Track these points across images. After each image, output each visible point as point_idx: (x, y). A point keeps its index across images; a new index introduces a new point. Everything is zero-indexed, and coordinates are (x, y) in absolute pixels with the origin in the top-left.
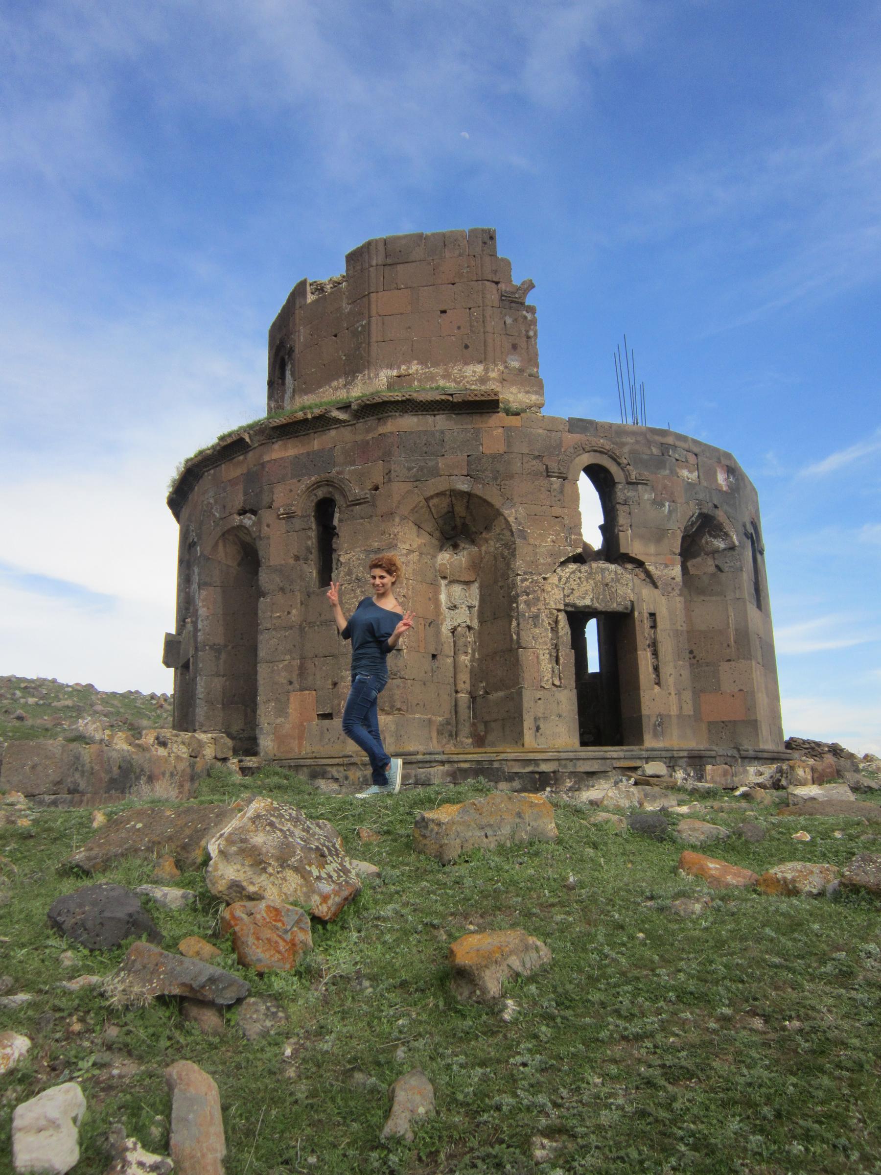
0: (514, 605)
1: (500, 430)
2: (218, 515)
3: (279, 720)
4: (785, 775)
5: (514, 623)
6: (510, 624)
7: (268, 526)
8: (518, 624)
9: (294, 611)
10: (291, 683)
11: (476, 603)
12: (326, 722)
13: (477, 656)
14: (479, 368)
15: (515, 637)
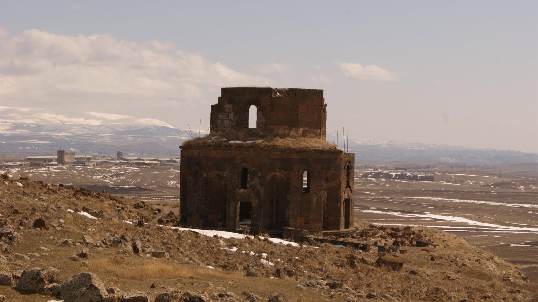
0: (339, 199)
1: (340, 159)
2: (269, 167)
3: (295, 224)
4: (364, 234)
5: (339, 204)
6: (338, 203)
7: (292, 176)
8: (340, 204)
9: (299, 198)
10: (298, 215)
11: (326, 196)
12: (307, 224)
13: (325, 208)
14: (320, 131)
15: (339, 207)
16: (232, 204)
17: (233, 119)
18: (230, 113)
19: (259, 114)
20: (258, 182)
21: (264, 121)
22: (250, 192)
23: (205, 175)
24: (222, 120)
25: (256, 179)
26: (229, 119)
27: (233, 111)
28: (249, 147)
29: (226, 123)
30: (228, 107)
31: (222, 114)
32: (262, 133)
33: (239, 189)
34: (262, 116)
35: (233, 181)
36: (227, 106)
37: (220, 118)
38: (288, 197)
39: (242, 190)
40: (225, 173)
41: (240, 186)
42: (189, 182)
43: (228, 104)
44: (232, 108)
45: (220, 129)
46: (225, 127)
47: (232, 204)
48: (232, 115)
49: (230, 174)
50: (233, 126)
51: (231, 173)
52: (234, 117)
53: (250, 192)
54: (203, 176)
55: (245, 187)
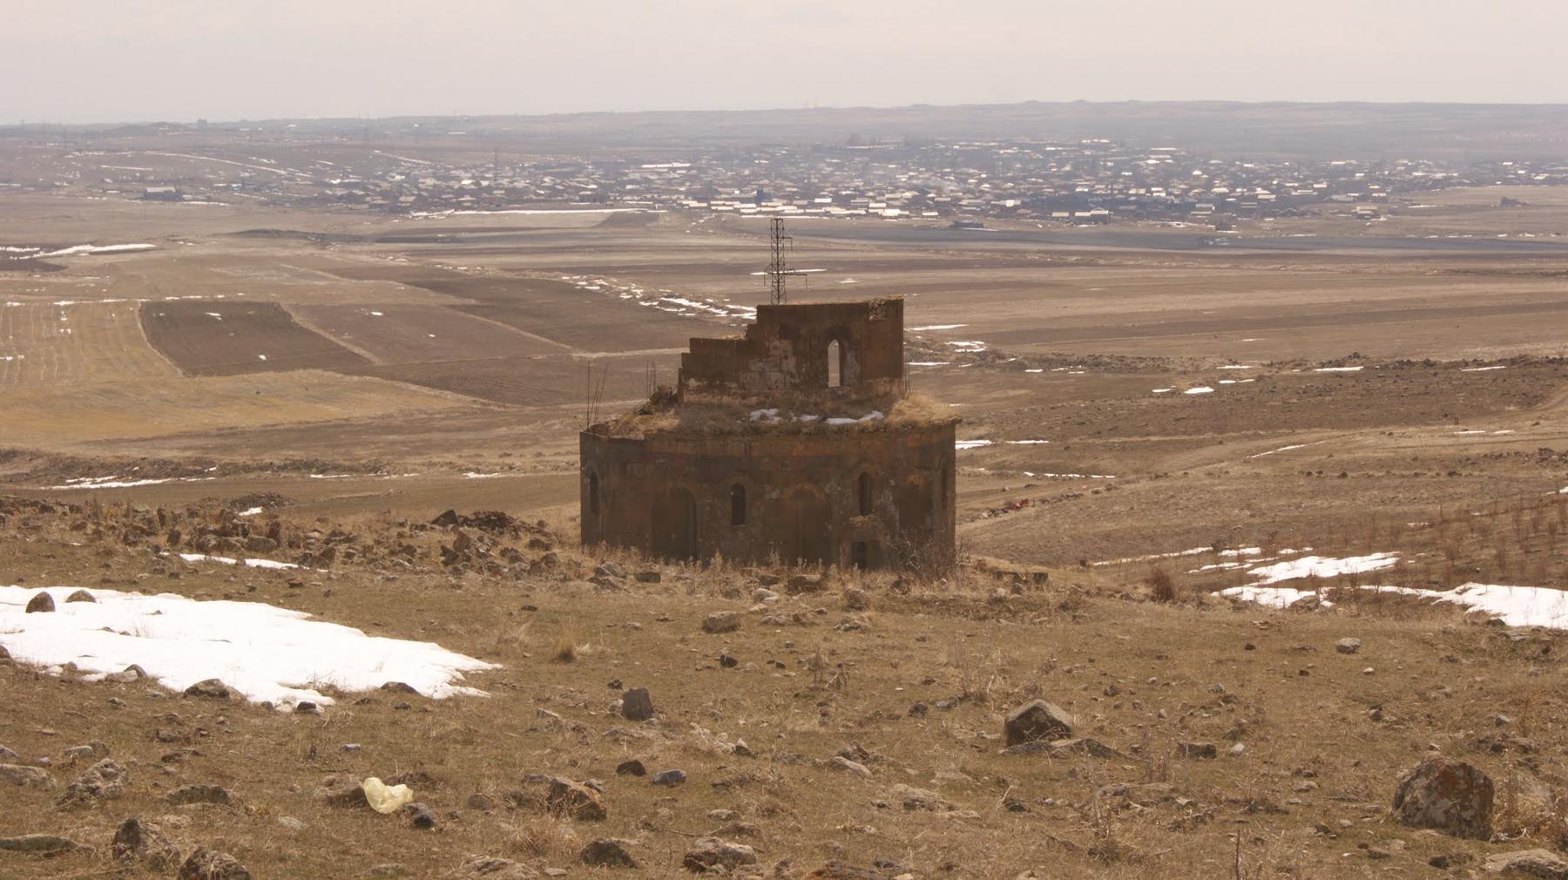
16: (844, 550)
17: (794, 371)
18: (786, 358)
19: (849, 356)
20: (891, 498)
21: (859, 370)
22: (875, 520)
23: (774, 495)
24: (761, 374)
25: (887, 492)
26: (781, 371)
27: (794, 354)
28: (877, 430)
29: (774, 379)
30: (779, 346)
31: (760, 361)
32: (854, 397)
33: (855, 516)
34: (853, 359)
35: (845, 502)
36: (777, 343)
37: (753, 368)
38: (928, 521)
39: (860, 518)
40: (828, 486)
41: (858, 511)
42: (708, 508)
43: (780, 338)
44: (790, 348)
45: (756, 391)
46: (770, 389)
47: (844, 550)
48: (791, 363)
49: (839, 489)
50: (795, 386)
51: (839, 485)
52: (798, 366)
53: (875, 520)
54: (767, 497)
55: (863, 513)
